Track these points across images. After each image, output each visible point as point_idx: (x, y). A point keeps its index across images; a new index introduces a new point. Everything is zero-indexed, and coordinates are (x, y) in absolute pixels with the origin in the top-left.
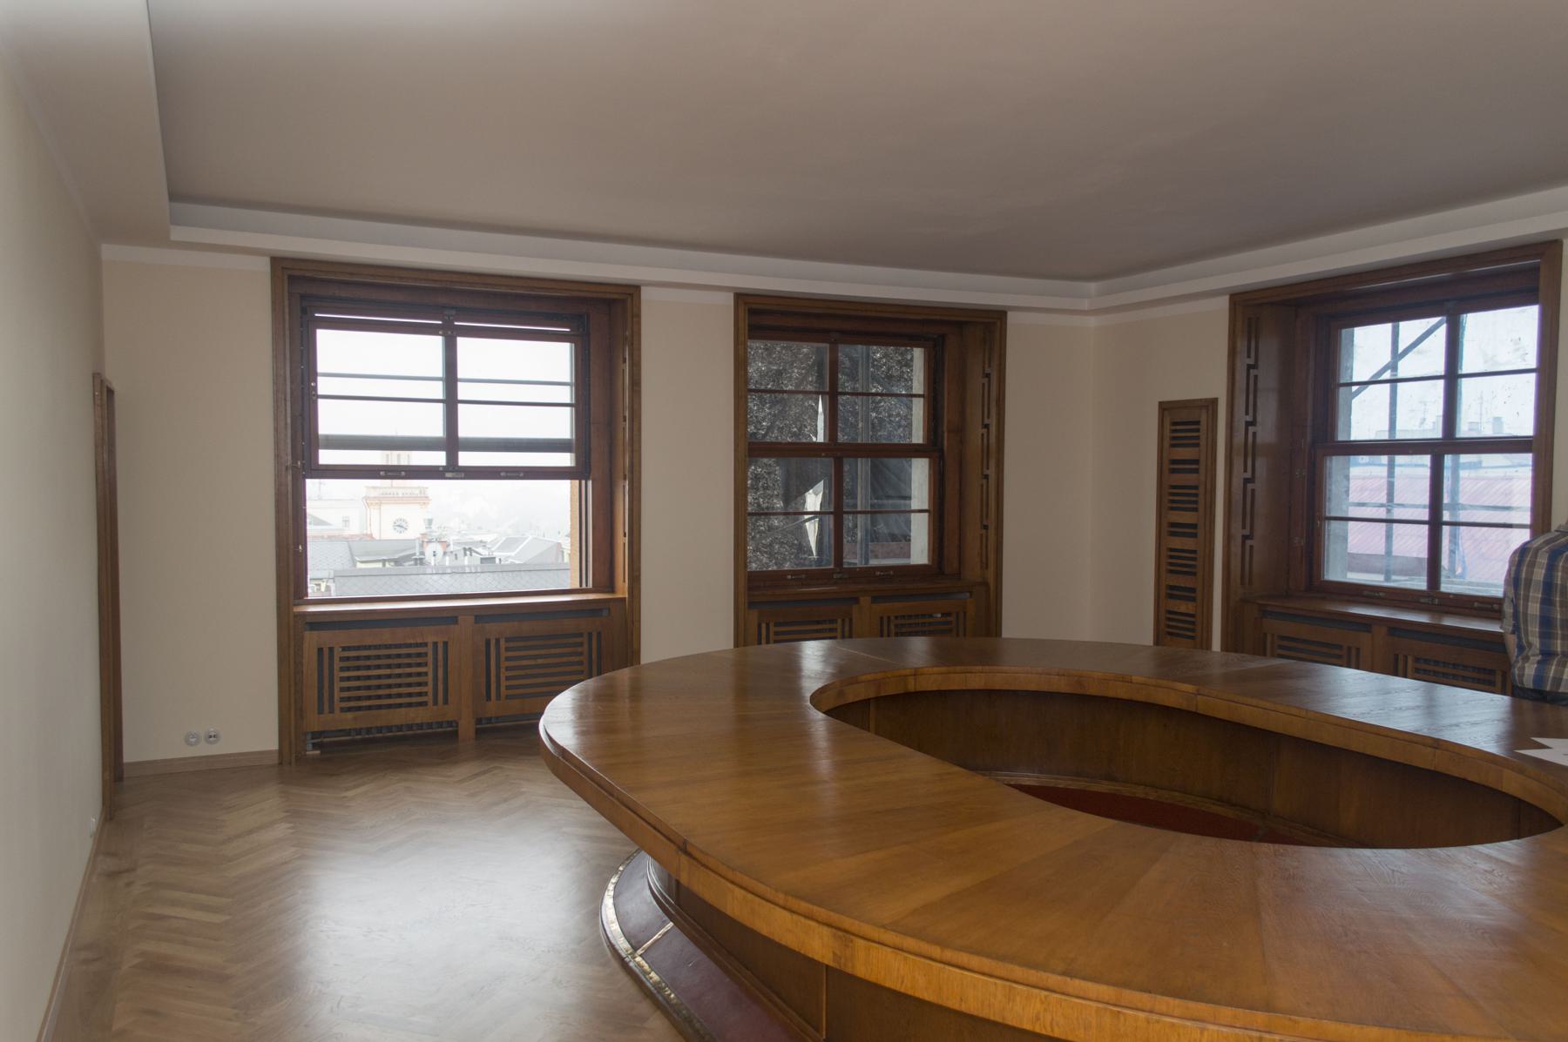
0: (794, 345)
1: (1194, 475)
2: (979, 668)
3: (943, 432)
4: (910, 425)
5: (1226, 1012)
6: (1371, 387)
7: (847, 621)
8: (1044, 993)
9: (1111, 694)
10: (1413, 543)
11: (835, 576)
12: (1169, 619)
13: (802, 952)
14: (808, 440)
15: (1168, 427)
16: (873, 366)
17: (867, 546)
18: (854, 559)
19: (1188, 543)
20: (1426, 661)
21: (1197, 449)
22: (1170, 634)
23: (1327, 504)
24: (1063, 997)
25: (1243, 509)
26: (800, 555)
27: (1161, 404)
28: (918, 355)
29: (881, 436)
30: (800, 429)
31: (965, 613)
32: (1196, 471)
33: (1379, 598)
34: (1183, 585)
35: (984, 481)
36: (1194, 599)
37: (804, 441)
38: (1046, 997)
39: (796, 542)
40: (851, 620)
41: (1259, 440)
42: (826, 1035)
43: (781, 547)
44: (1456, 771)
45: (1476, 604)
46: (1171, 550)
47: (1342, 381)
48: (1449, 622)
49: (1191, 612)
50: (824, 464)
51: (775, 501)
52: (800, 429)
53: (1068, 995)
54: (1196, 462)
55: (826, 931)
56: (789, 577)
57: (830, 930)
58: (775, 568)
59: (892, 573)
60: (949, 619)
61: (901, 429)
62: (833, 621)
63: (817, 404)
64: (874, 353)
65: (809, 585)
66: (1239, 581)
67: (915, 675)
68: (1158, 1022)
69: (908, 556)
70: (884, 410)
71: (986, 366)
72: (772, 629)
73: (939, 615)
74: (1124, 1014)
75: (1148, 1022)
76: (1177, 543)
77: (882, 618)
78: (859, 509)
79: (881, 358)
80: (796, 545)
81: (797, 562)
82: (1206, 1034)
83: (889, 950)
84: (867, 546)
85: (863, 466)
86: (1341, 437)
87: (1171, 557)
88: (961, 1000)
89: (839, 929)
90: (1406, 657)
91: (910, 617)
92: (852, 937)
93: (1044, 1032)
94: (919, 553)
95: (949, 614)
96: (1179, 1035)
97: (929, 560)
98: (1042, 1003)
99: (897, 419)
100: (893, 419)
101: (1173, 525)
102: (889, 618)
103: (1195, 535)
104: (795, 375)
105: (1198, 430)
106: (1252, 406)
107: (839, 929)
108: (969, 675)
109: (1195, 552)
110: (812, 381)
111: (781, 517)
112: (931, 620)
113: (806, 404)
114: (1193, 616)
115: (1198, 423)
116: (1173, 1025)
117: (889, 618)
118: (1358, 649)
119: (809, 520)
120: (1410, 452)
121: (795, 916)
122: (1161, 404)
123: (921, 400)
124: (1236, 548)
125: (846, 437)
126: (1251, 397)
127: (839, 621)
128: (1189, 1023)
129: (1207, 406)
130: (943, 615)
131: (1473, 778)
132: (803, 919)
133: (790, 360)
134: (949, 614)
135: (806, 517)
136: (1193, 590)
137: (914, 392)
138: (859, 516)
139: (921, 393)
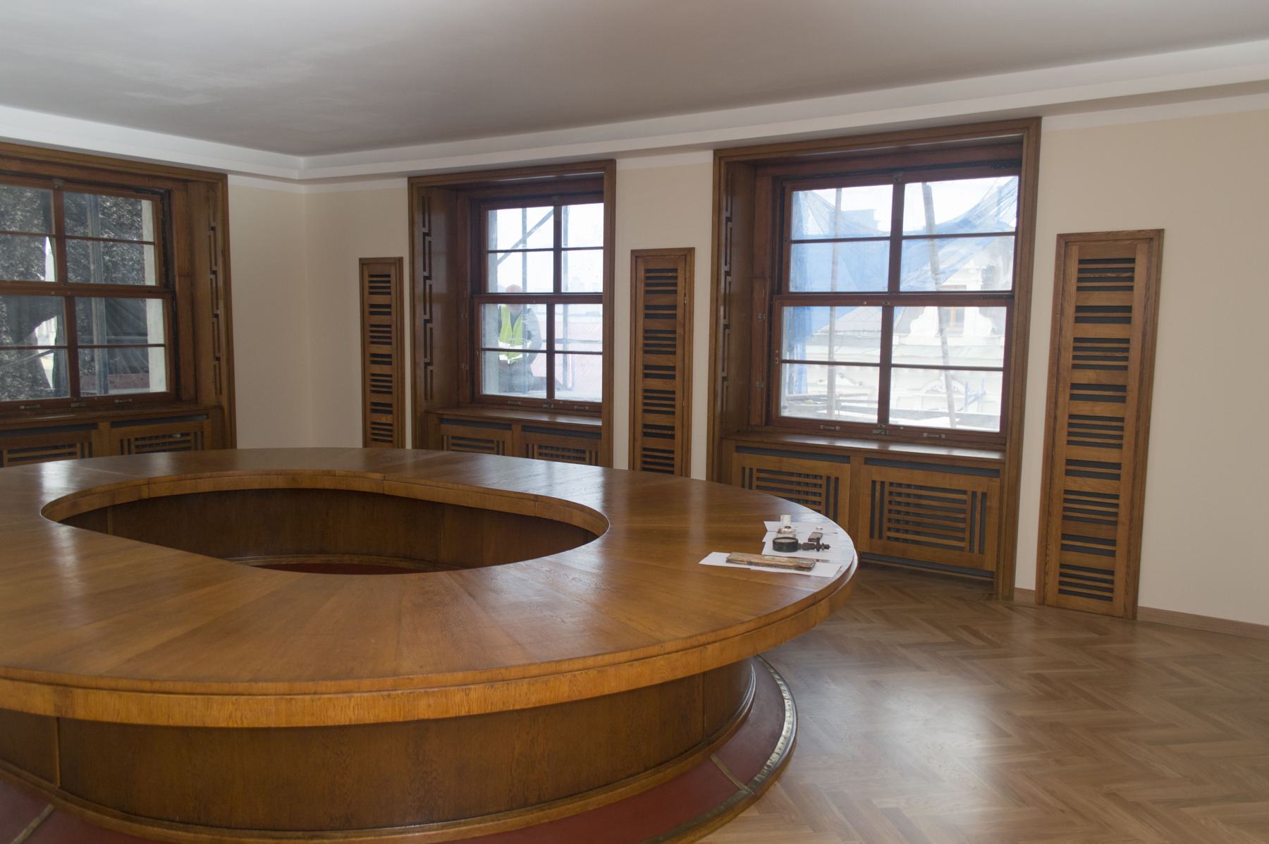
0: (16, 189)
1: (388, 317)
2: (209, 474)
3: (174, 276)
4: (143, 269)
5: (367, 683)
6: (513, 254)
7: (86, 445)
8: (235, 698)
9: (320, 486)
10: (539, 366)
11: (73, 405)
12: (374, 429)
13: (25, 710)
14: (36, 279)
15: (367, 279)
16: (103, 214)
17: (105, 377)
18: (91, 388)
19: (385, 369)
20: (546, 447)
21: (389, 296)
22: (375, 440)
23: (483, 339)
24: (250, 697)
25: (424, 343)
26: (35, 387)
27: (361, 260)
28: (146, 207)
29: (115, 277)
30: (27, 269)
31: (202, 432)
32: (389, 313)
33: (518, 405)
34: (383, 402)
35: (215, 320)
36: (391, 412)
37: (32, 280)
38: (236, 700)
39: (30, 375)
40: (90, 444)
41: (434, 291)
42: (61, 783)
43: (14, 380)
44: (547, 515)
45: (576, 407)
46: (373, 375)
47: (490, 249)
48: (562, 420)
49: (389, 422)
50: (58, 301)
51: (4, 337)
52: (27, 269)
53: (254, 695)
54: (389, 306)
55: (47, 689)
56: (23, 407)
57: (51, 687)
58: (8, 400)
59: (130, 400)
60: (189, 438)
61: (135, 272)
62: (71, 446)
63: (44, 245)
64: (104, 202)
65: (45, 414)
66: (423, 397)
67: (148, 484)
68: (319, 699)
69: (147, 385)
70: (117, 254)
71: (211, 220)
73: (179, 436)
74: (295, 699)
75: (313, 701)
76: (377, 369)
77: (122, 441)
78: (95, 343)
79: (111, 207)
80: (30, 378)
81: (32, 394)
82: (353, 700)
83: (105, 692)
84: (105, 377)
85: (98, 306)
86: (491, 290)
87: (373, 380)
88: (169, 717)
89: (58, 685)
90: (533, 446)
91: (150, 438)
92: (71, 689)
93: (235, 726)
94: (158, 382)
95: (188, 434)
96: (334, 705)
97: (167, 389)
98: (233, 704)
99: (131, 263)
100: (126, 263)
101: (374, 355)
102: (129, 440)
103: (390, 363)
104: (19, 215)
105: (389, 282)
106: (428, 265)
107: (58, 685)
108: (198, 480)
109: (390, 376)
110: (38, 225)
111: (13, 352)
112: (171, 440)
113: (33, 246)
114: (391, 425)
115: (389, 276)
116: (330, 699)
117: (129, 440)
118: (504, 442)
119: (43, 355)
120: (534, 301)
121: (17, 683)
122: (361, 260)
123: (152, 247)
124: (420, 373)
125: (79, 278)
126: (427, 257)
127: (78, 445)
128: (341, 696)
129: (395, 264)
130: (182, 435)
131: (557, 518)
132: (24, 684)
133: (12, 202)
134: (188, 434)
135: (40, 351)
136: (390, 405)
137: (145, 239)
138: (96, 350)
139: (151, 240)
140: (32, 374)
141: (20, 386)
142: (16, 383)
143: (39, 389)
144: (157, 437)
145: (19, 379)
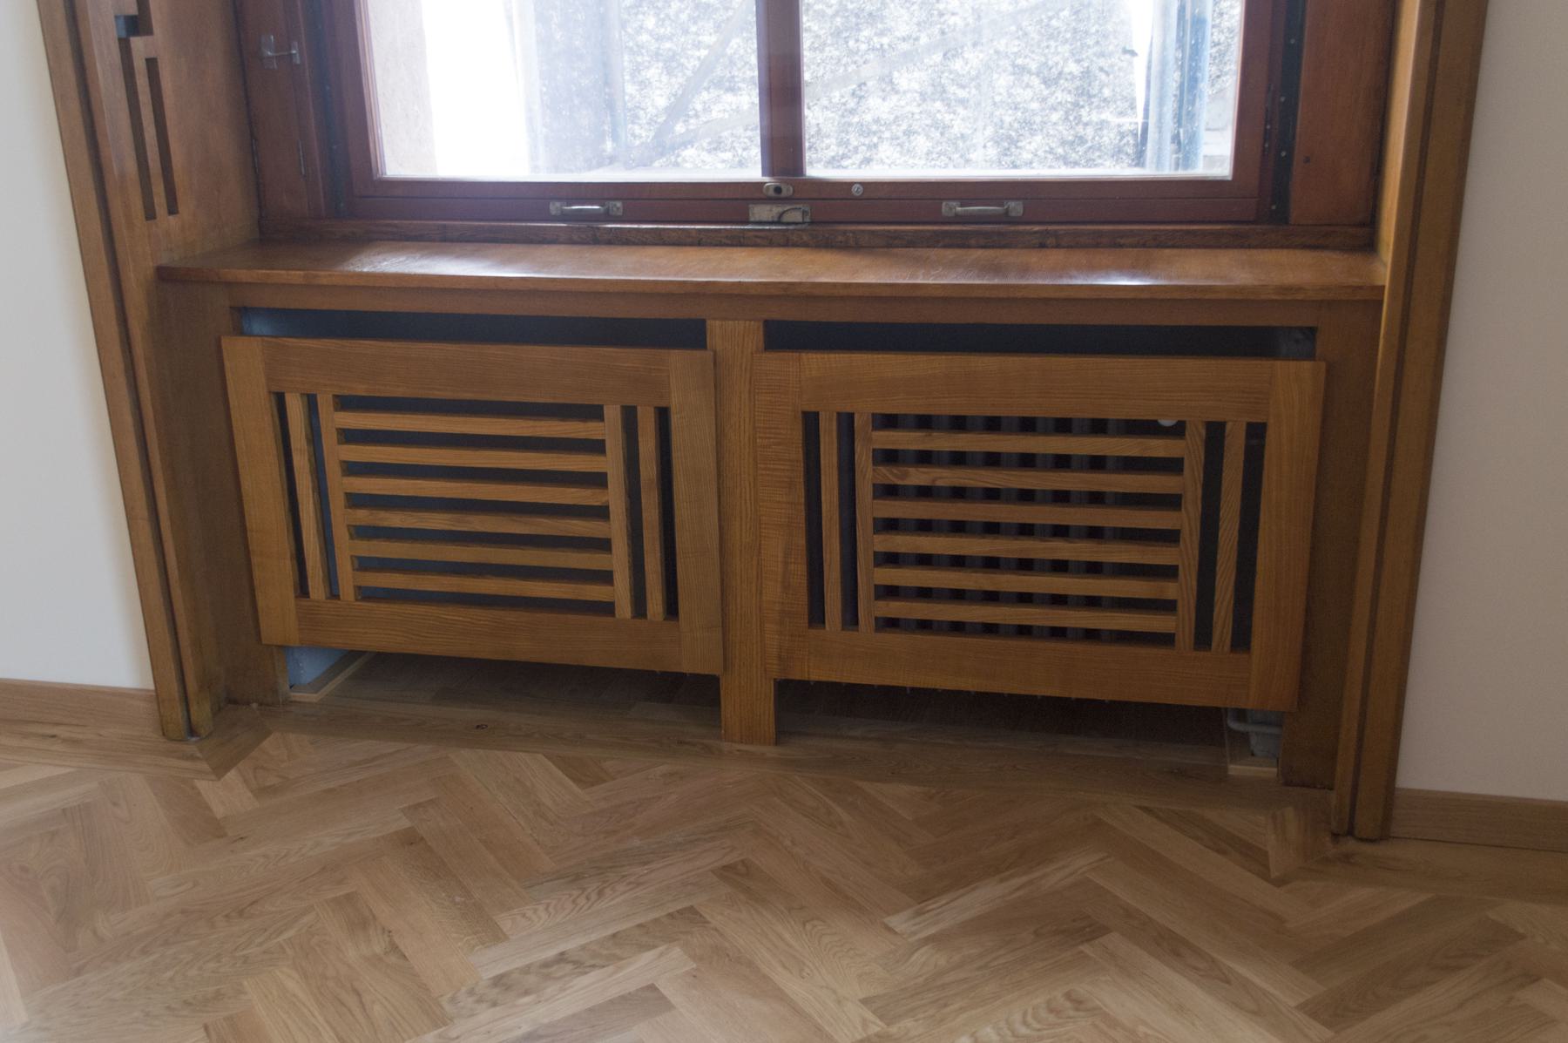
11: (762, 212)
26: (1084, 112)
39: (1072, 67)
59: (1016, 208)
62: (595, 413)
72: (335, 420)
77: (811, 422)
102: (847, 423)
117: (847, 423)
127: (613, 413)
140: (1078, 61)
141: (1035, 105)
142: (1024, 95)
143: (1095, 117)
144: (959, 424)
145: (1035, 81)
